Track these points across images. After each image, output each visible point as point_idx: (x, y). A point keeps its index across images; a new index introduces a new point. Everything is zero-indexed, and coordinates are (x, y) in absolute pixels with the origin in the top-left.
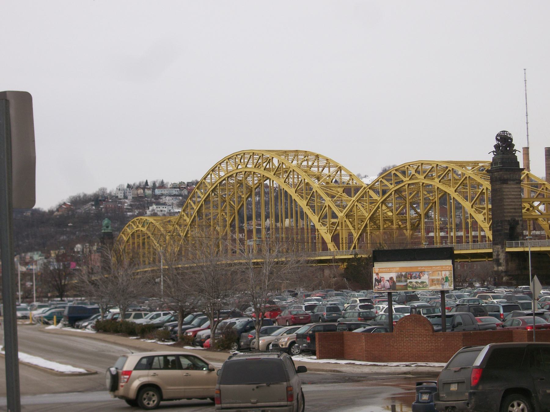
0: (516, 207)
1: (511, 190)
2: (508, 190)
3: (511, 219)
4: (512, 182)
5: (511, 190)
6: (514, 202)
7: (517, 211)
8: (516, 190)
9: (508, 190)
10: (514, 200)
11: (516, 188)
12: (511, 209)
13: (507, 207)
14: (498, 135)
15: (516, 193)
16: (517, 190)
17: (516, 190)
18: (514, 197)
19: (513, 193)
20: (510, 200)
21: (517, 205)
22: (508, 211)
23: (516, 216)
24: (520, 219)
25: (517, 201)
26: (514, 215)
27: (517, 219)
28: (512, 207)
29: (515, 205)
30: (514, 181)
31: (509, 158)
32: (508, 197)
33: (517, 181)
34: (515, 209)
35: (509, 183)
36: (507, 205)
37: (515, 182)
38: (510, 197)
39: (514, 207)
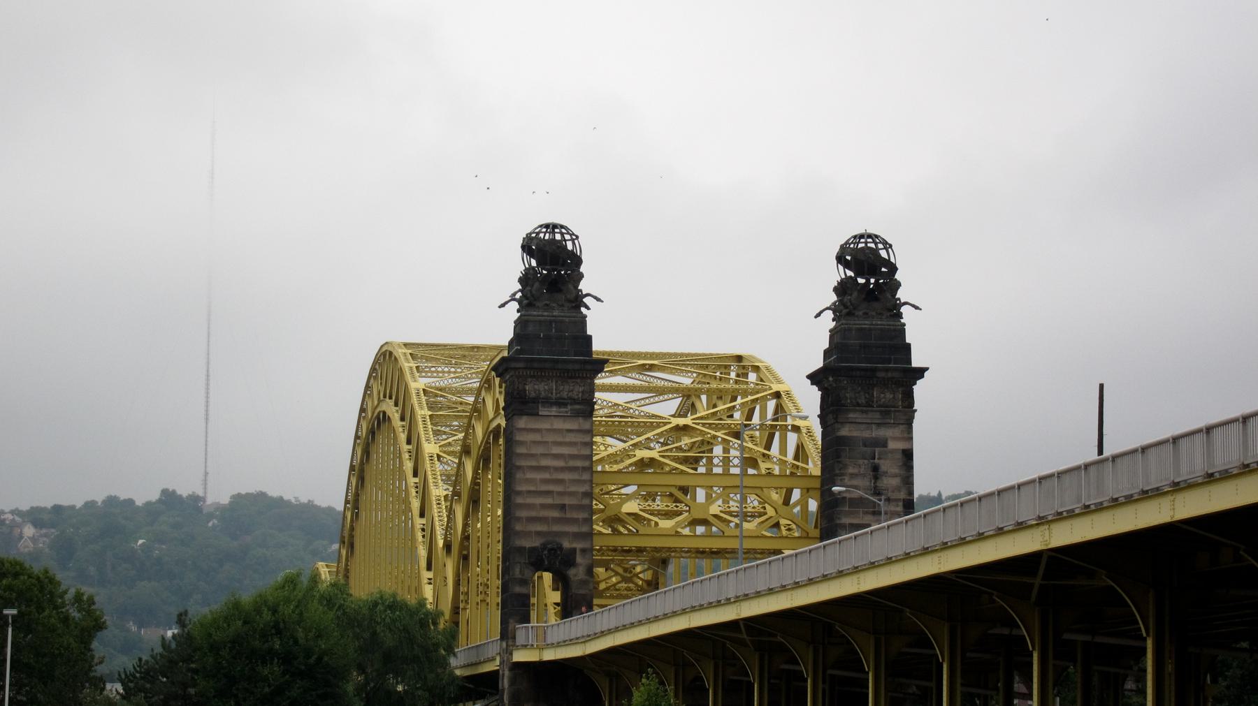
0: (567, 501)
1: (550, 438)
2: (537, 437)
3: (544, 546)
4: (554, 410)
5: (550, 438)
7: (568, 515)
8: (570, 438)
9: (537, 437)
10: (566, 476)
12: (543, 506)
13: (530, 500)
14: (844, 249)
15: (573, 451)
16: (574, 440)
17: (570, 438)
18: (561, 463)
19: (556, 450)
20: (547, 476)
21: (571, 494)
22: (533, 514)
23: (566, 534)
24: (578, 545)
26: (556, 528)
27: (566, 545)
28: (549, 501)
29: (561, 494)
30: (565, 405)
31: (551, 322)
32: (534, 463)
33: (577, 407)
34: (563, 507)
35: (543, 411)
36: (529, 492)
37: (569, 407)
38: (544, 462)
39: (558, 501)
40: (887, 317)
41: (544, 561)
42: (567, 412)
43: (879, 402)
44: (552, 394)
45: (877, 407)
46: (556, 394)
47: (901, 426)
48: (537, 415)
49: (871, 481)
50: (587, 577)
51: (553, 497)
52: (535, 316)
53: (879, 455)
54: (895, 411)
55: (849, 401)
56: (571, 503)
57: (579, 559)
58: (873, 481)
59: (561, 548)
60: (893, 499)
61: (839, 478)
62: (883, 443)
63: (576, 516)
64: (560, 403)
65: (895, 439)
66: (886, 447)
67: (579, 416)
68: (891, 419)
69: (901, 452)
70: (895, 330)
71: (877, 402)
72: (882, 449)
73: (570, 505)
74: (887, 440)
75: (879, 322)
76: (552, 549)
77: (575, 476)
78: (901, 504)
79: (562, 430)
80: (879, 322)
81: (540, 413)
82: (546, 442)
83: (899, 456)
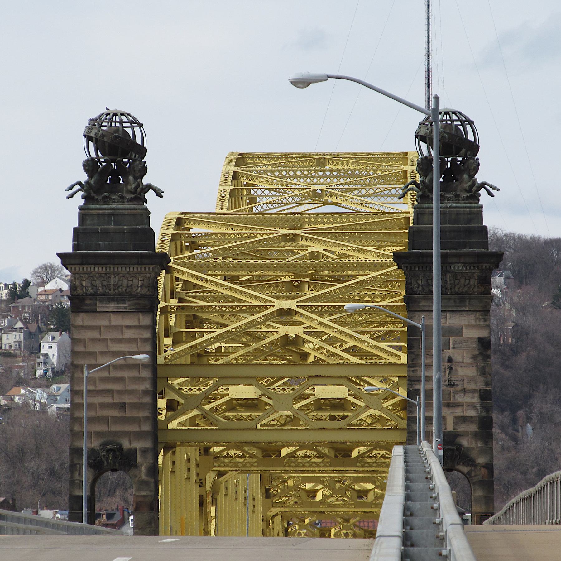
0: (127, 399)
1: (109, 335)
2: (95, 334)
3: (104, 445)
4: (112, 306)
5: (109, 335)
6: (121, 380)
7: (128, 414)
8: (129, 334)
9: (95, 334)
10: (126, 374)
11: (128, 327)
16: (133, 336)
17: (129, 334)
21: (131, 392)
23: (127, 434)
24: (138, 445)
25: (129, 378)
26: (115, 428)
27: (126, 444)
28: (107, 400)
29: (119, 392)
34: (123, 406)
35: (101, 307)
39: (117, 400)
40: (464, 199)
41: (103, 462)
42: (126, 308)
43: (453, 290)
44: (110, 290)
45: (451, 294)
46: (114, 290)
47: (478, 314)
48: (96, 312)
49: (445, 372)
50: (147, 478)
51: (113, 396)
52: (93, 209)
53: (454, 344)
54: (470, 298)
55: (420, 289)
56: (131, 401)
57: (139, 459)
58: (448, 372)
59: (120, 449)
60: (468, 390)
61: (413, 369)
62: (458, 332)
63: (136, 415)
64: (119, 298)
65: (470, 326)
66: (462, 336)
67: (139, 312)
68: (465, 306)
69: (476, 340)
70: (470, 213)
71: (451, 289)
72: (457, 338)
73: (129, 404)
74: (462, 329)
75: (454, 205)
76: (111, 450)
77: (135, 374)
78: (477, 395)
79: (122, 326)
80: (454, 205)
81: (98, 311)
82: (106, 340)
83: (474, 345)
